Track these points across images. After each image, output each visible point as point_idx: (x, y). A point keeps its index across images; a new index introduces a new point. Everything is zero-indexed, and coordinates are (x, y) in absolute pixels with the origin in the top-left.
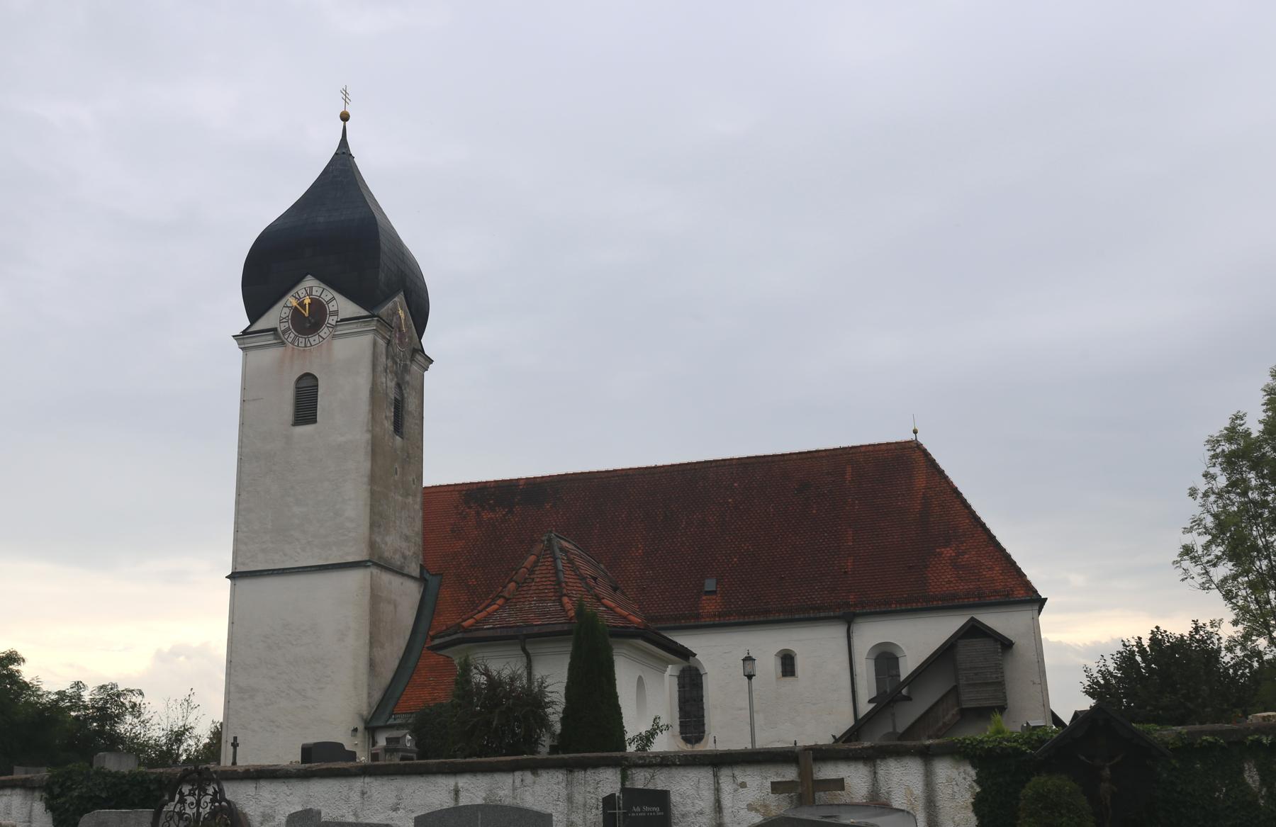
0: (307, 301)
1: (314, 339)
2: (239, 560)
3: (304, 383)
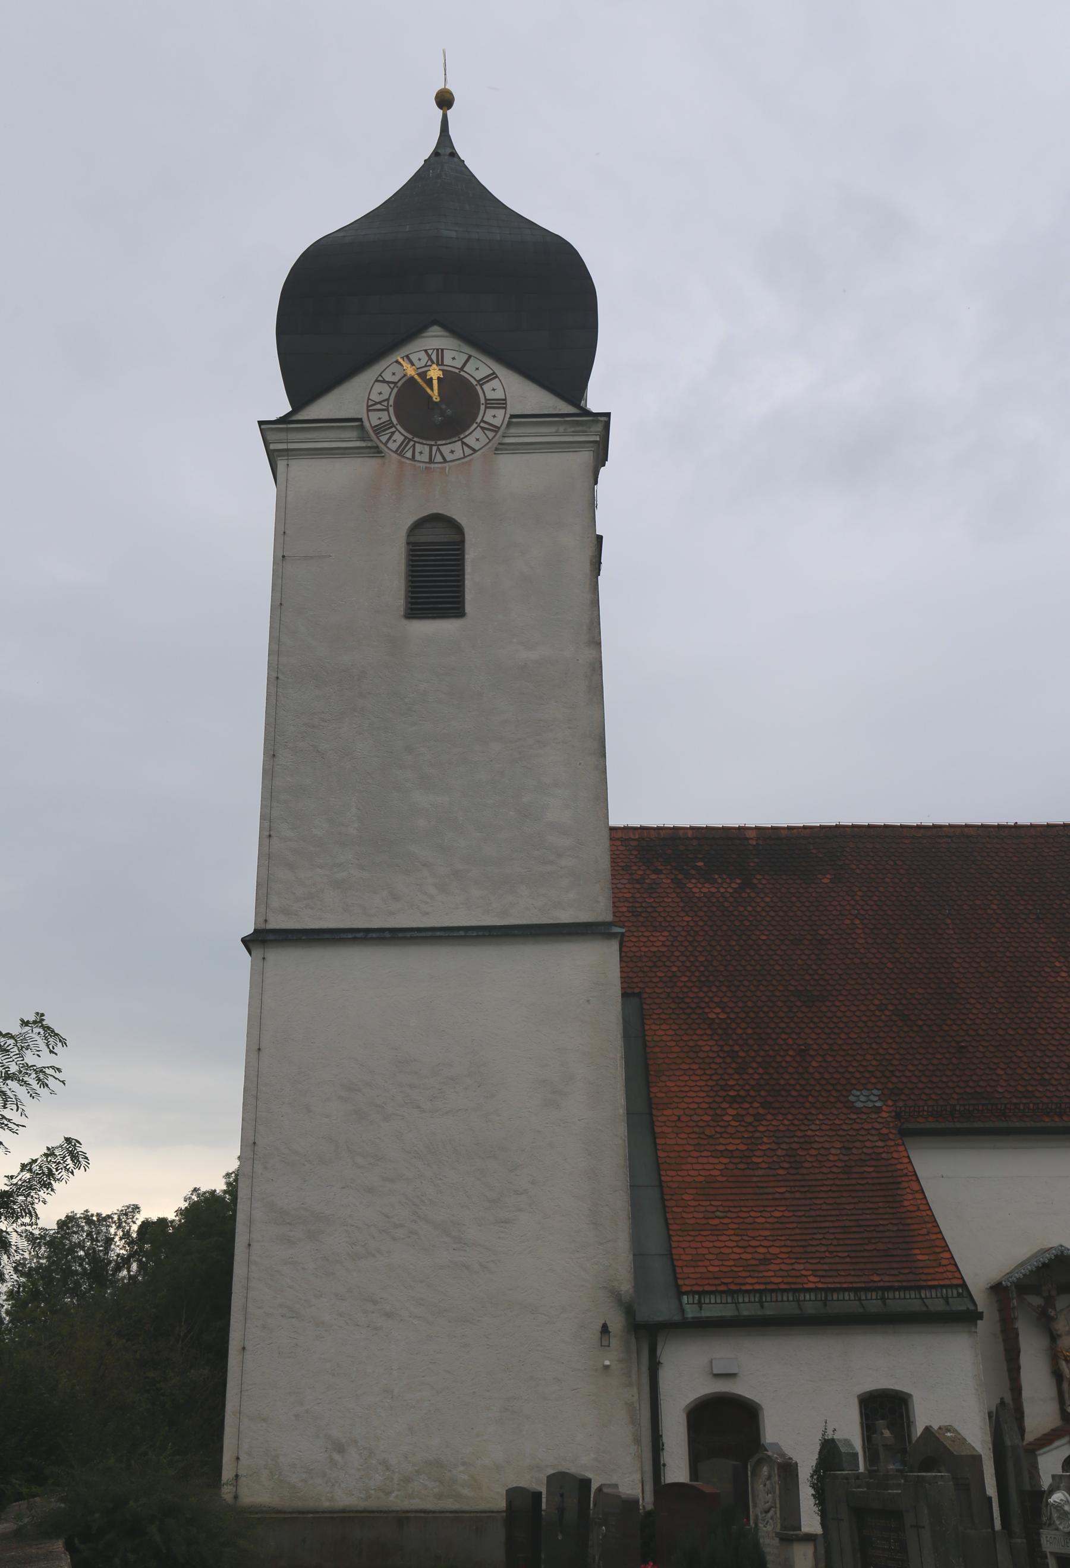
0: (435, 373)
1: (452, 450)
2: (275, 902)
3: (428, 536)
